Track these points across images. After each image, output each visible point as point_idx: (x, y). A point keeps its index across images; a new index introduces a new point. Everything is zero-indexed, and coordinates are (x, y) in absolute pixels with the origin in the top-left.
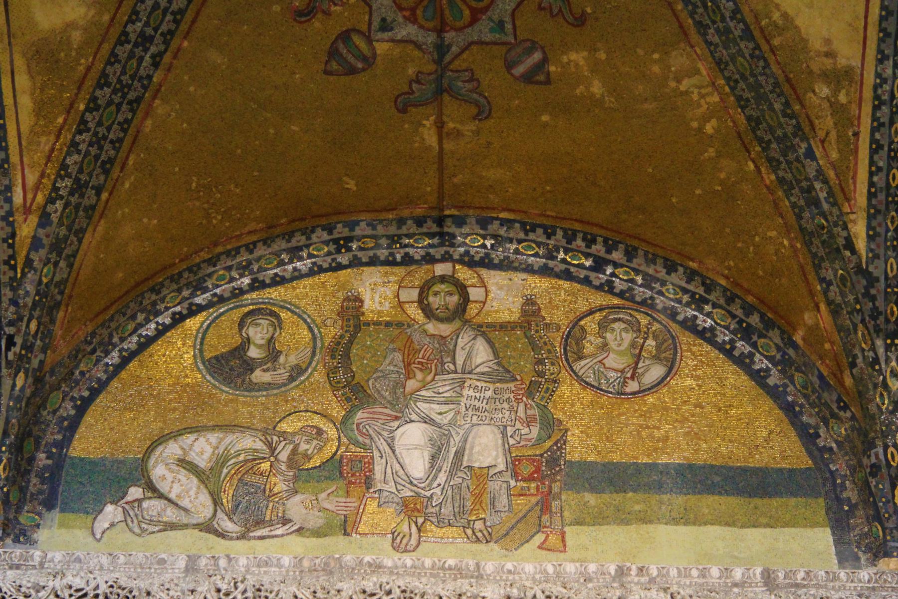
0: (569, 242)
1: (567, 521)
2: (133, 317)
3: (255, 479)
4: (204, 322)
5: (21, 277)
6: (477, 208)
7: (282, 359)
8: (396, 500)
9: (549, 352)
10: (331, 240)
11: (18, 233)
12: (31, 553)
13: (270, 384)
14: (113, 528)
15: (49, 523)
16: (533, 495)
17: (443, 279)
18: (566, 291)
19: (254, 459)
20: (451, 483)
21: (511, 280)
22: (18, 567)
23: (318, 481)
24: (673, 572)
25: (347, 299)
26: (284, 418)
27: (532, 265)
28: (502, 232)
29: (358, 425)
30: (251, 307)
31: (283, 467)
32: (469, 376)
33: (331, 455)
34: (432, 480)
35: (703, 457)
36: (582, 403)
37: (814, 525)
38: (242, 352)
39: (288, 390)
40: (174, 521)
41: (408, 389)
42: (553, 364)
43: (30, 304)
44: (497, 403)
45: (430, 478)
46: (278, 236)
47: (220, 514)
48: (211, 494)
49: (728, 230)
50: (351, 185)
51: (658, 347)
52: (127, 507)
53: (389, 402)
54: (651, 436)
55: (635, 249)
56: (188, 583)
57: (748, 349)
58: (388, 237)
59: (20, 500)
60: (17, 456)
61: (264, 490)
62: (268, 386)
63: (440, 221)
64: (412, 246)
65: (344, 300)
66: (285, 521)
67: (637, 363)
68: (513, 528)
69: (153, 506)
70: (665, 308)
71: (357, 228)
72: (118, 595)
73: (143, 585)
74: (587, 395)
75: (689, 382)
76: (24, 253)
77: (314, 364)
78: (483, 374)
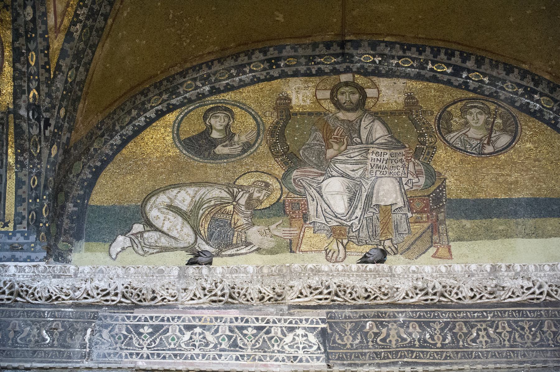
0: (435, 57)
1: (452, 238)
2: (129, 112)
4: (179, 116)
5: (54, 77)
6: (369, 34)
7: (236, 138)
8: (326, 228)
9: (427, 128)
10: (267, 60)
11: (51, 46)
12: (67, 267)
13: (229, 155)
15: (78, 248)
16: (425, 222)
17: (347, 84)
18: (435, 89)
19: (222, 203)
20: (365, 216)
21: (395, 83)
22: (59, 277)
23: (269, 217)
24: (532, 268)
25: (280, 98)
26: (241, 176)
27: (409, 74)
28: (387, 51)
30: (211, 106)
35: (544, 194)
36: (454, 161)
40: (167, 245)
42: (431, 136)
43: (60, 97)
44: (394, 162)
45: (350, 213)
46: (229, 56)
47: (200, 241)
48: (192, 228)
49: (550, 38)
50: (280, 18)
51: (504, 123)
52: (133, 237)
53: (315, 164)
54: (506, 182)
55: (483, 58)
56: (182, 284)
58: (306, 57)
59: (57, 233)
60: (54, 203)
61: (230, 224)
62: (227, 156)
63: (342, 45)
64: (323, 63)
65: (277, 99)
66: (247, 244)
67: (490, 134)
68: (412, 244)
69: (151, 236)
70: (506, 98)
71: (284, 51)
72: (132, 293)
73: (148, 286)
74: (458, 156)
75: (529, 145)
76: (56, 60)
77: (259, 141)
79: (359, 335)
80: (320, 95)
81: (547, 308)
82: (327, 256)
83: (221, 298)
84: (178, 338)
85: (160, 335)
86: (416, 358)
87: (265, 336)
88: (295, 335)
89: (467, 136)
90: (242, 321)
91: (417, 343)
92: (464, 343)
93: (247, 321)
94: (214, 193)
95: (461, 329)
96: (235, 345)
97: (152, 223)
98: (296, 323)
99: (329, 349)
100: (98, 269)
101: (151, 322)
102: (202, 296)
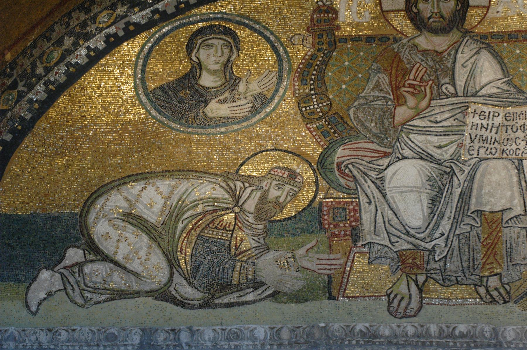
2: (60, 42)
3: (217, 235)
7: (242, 87)
8: (390, 255)
13: (228, 118)
14: (50, 298)
20: (457, 232)
23: (294, 235)
25: (318, 10)
26: (249, 158)
29: (339, 165)
30: (200, 24)
31: (251, 219)
32: (473, 99)
33: (307, 202)
34: (433, 229)
38: (193, 82)
39: (252, 125)
41: (398, 119)
44: (510, 132)
47: (177, 278)
53: (375, 135)
61: (229, 247)
62: (226, 121)
65: (314, 11)
66: (257, 285)
77: (281, 91)
82: (389, 306)
94: (202, 191)
97: (99, 249)
100: (7, 335)
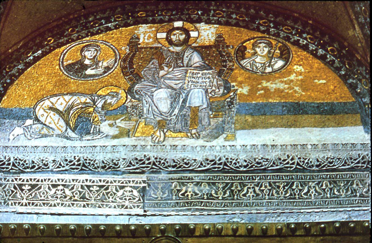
7: (100, 64)
9: (228, 57)
17: (178, 28)
25: (132, 38)
31: (100, 110)
32: (190, 68)
37: (356, 125)
42: (230, 61)
47: (69, 130)
51: (281, 54)
52: (25, 128)
57: (324, 52)
65: (131, 39)
67: (271, 60)
77: (116, 65)
78: (197, 67)
79: (167, 191)
80: (159, 36)
81: (297, 174)
83: (78, 167)
84: (47, 193)
85: (36, 190)
86: (203, 206)
87: (104, 192)
88: (124, 191)
89: (255, 61)
90: (90, 182)
91: (205, 197)
92: (237, 196)
93: (93, 182)
95: (237, 187)
96: (83, 198)
98: (126, 183)
99: (146, 200)
101: (30, 182)
102: (65, 165)
